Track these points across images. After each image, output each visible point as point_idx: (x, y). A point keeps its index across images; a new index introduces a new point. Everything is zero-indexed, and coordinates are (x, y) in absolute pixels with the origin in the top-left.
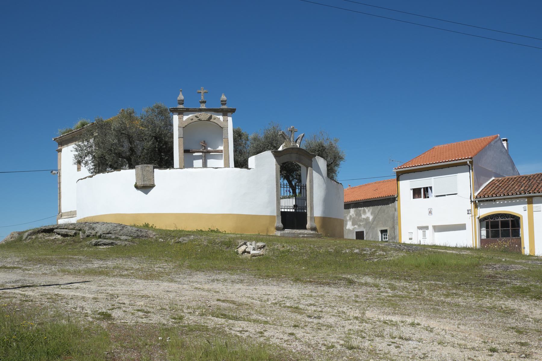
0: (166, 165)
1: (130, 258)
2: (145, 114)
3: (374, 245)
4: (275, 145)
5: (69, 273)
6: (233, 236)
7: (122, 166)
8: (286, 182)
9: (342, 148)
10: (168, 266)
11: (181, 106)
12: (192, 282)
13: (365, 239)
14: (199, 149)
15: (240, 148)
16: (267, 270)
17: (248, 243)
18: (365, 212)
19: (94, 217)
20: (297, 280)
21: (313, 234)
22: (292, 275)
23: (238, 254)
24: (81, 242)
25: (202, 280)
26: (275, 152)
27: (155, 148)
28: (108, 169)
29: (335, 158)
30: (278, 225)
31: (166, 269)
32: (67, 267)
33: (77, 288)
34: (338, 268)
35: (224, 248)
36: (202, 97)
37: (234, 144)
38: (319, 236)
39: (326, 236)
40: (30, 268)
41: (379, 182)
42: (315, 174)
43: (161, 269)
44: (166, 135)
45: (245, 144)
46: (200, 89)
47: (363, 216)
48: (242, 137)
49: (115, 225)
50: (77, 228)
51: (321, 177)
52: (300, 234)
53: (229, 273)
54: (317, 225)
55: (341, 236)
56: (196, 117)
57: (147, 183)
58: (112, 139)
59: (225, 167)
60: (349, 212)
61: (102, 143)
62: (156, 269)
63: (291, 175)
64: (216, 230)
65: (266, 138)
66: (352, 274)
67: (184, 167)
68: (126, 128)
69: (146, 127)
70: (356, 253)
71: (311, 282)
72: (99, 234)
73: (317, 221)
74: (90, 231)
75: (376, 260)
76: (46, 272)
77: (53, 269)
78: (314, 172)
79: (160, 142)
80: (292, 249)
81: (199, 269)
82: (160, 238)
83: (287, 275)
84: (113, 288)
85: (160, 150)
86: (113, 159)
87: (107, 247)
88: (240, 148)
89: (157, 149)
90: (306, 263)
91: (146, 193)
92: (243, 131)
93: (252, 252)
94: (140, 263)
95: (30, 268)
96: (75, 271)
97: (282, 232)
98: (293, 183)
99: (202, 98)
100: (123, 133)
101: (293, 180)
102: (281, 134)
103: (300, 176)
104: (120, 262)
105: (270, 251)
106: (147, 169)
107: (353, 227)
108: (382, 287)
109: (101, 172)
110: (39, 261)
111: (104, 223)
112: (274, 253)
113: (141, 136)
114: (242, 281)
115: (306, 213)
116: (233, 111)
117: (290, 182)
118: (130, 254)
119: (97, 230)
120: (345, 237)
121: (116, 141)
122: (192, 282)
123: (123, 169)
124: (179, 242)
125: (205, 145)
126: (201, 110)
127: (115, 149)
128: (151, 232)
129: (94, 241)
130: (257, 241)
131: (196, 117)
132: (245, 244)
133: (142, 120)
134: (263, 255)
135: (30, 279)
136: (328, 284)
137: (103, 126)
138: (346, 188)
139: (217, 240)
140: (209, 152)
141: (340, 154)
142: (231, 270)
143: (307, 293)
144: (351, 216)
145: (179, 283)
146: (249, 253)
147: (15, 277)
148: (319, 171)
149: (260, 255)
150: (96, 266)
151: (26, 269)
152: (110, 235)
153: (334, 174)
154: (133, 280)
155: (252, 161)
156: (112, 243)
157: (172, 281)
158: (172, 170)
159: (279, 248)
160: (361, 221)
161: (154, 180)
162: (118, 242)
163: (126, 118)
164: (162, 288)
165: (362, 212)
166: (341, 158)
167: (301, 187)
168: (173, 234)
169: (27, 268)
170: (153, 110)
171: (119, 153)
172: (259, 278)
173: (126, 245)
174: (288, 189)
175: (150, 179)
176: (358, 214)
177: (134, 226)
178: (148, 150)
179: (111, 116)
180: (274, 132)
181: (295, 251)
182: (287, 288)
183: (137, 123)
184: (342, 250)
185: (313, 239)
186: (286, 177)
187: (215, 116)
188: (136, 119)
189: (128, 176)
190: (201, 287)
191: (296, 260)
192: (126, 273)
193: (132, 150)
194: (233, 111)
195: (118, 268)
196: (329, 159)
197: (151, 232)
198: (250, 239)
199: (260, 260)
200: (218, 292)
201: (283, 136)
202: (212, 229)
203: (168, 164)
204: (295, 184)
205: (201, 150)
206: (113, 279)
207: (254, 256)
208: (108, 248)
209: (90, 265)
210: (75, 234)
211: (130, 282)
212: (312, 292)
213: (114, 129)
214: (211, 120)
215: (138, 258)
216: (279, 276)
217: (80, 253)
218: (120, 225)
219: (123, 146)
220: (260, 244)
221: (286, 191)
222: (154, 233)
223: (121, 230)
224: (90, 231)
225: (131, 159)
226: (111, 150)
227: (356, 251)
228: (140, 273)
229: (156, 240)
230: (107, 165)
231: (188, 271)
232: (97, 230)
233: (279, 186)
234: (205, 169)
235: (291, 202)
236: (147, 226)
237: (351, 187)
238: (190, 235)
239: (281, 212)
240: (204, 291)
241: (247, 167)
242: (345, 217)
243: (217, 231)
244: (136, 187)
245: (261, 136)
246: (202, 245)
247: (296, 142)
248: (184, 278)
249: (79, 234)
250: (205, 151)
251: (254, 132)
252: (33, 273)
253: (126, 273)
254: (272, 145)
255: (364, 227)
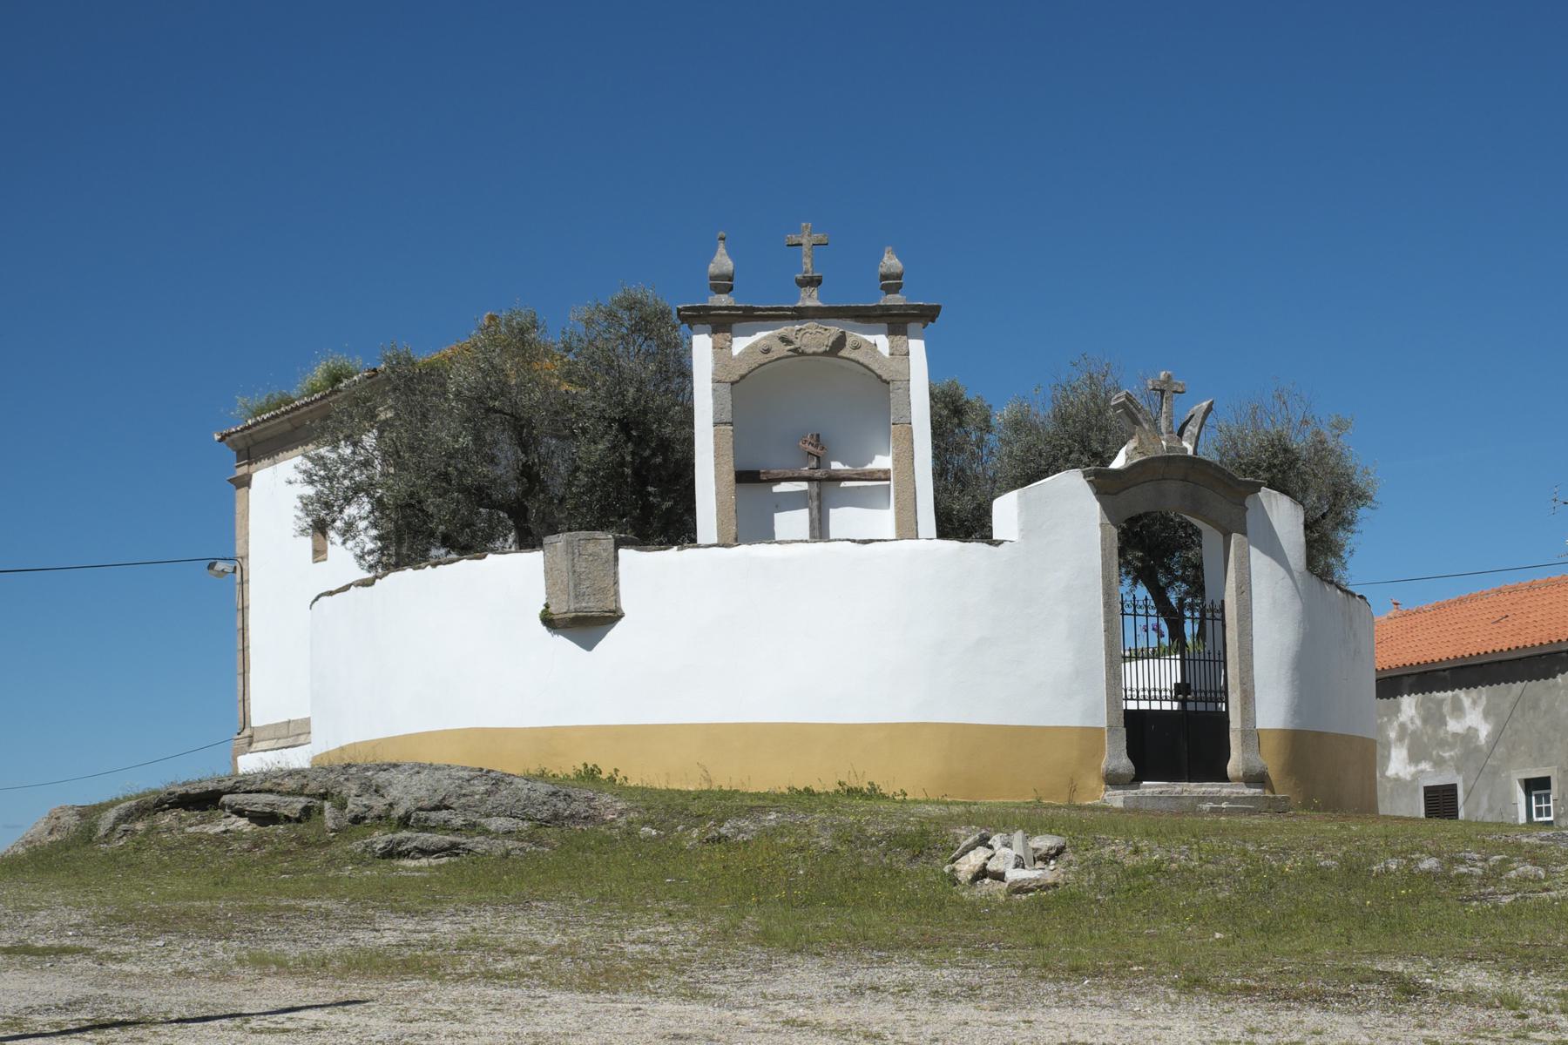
0: (663, 531)
1: (524, 903)
2: (581, 329)
3: (1502, 841)
4: (1096, 446)
5: (283, 967)
6: (934, 810)
7: (490, 538)
8: (1142, 592)
9: (1362, 456)
10: (678, 936)
11: (724, 300)
12: (775, 997)
13: (1462, 814)
14: (795, 471)
15: (958, 460)
16: (1072, 944)
17: (996, 840)
18: (1458, 709)
19: (379, 742)
20: (1194, 984)
21: (1253, 798)
22: (1175, 963)
23: (955, 882)
24: (329, 843)
25: (815, 990)
26: (1097, 474)
27: (622, 464)
28: (434, 552)
29: (1337, 494)
30: (1114, 764)
31: (671, 949)
32: (275, 946)
33: (316, 1029)
34: (1357, 934)
35: (901, 860)
36: (807, 264)
37: (935, 447)
38: (1278, 808)
39: (1305, 806)
40: (125, 949)
41: (1515, 589)
42: (1259, 561)
43: (648, 948)
44: (663, 412)
45: (980, 443)
46: (798, 231)
47: (1454, 726)
48: (966, 418)
49: (465, 774)
50: (313, 787)
51: (1281, 571)
52: (1202, 799)
53: (923, 961)
54: (1270, 761)
55: (1366, 806)
56: (785, 340)
57: (592, 605)
58: (450, 434)
59: (901, 537)
60: (1398, 710)
61: (412, 449)
62: (630, 949)
63: (1163, 565)
64: (866, 786)
65: (1062, 419)
66: (1414, 957)
67: (738, 541)
68: (504, 389)
69: (584, 382)
70: (1429, 872)
71: (1248, 991)
72: (399, 811)
73: (1269, 745)
74: (365, 800)
75: (1507, 900)
76: (190, 965)
77: (220, 954)
78: (1254, 552)
79: (641, 442)
80: (1172, 860)
81: (801, 946)
82: (644, 824)
83: (1153, 964)
84: (457, 1026)
85: (642, 474)
86: (455, 513)
87: (434, 862)
88: (958, 460)
89: (628, 471)
90: (1229, 914)
91: (589, 646)
92: (969, 395)
93: (1013, 875)
94: (563, 925)
95: (125, 949)
96: (305, 962)
97: (1131, 793)
98: (1173, 598)
99: (807, 267)
100: (490, 407)
101: (1170, 584)
102: (1122, 405)
103: (1199, 567)
104: (484, 921)
105: (1085, 868)
106: (591, 547)
107: (1412, 769)
108: (1533, 1006)
109: (408, 565)
110: (164, 923)
111: (419, 768)
112: (1099, 877)
113: (564, 420)
114: (971, 993)
115: (1224, 718)
116: (927, 314)
117: (1159, 594)
118: (526, 889)
119: (394, 793)
120: (1384, 808)
121: (465, 440)
122: (775, 997)
123: (494, 551)
124: (719, 839)
125: (819, 449)
126: (801, 314)
127: (462, 473)
128: (606, 798)
129: (380, 839)
130: (1032, 830)
131: (785, 340)
132: (984, 841)
133: (570, 357)
134: (1055, 885)
135: (127, 993)
136: (1319, 999)
137: (411, 384)
138: (1382, 613)
139: (870, 830)
140: (837, 478)
141: (1356, 480)
142: (929, 947)
143: (1234, 1037)
144: (1403, 726)
145: (723, 1001)
146: (999, 876)
147: (68, 989)
148: (1273, 549)
149: (1045, 887)
150: (390, 938)
151: (111, 957)
152: (444, 814)
153: (1332, 560)
154: (539, 991)
155: (1006, 510)
156: (454, 845)
157: (693, 994)
158: (689, 553)
159: (1119, 857)
160: (1442, 744)
161: (617, 593)
162: (479, 844)
163: (505, 349)
164: (653, 1022)
165: (1446, 709)
166: (1360, 497)
167: (1203, 613)
168: (696, 807)
169: (115, 950)
170: (611, 315)
171: (480, 489)
172: (1043, 978)
173: (508, 853)
174: (1152, 621)
175: (603, 590)
176: (1434, 718)
177: (542, 776)
178: (593, 472)
179: (447, 340)
180: (1094, 396)
181: (1183, 870)
182: (1154, 1015)
183: (549, 368)
184: (1372, 863)
185: (1256, 820)
186: (1144, 575)
187: (854, 336)
188: (546, 353)
189: (514, 578)
190: (810, 1016)
191: (1190, 905)
192: (509, 963)
193: (528, 474)
194: (927, 314)
195: (478, 945)
196: (1312, 498)
197: (606, 798)
198: (1004, 821)
199: (1043, 906)
200: (878, 1036)
201: (1130, 411)
202: (854, 784)
203: (673, 527)
204: (1181, 600)
205: (805, 470)
206: (457, 992)
207: (1019, 888)
208: (439, 867)
209: (364, 937)
210: (307, 811)
211: (524, 1002)
212: (1252, 1031)
213: (458, 394)
214: (843, 353)
215: (556, 906)
216: (1120, 971)
217: (325, 887)
218: (484, 773)
219: (492, 460)
220: (1044, 842)
221: (1146, 628)
222: (620, 806)
223: (488, 793)
224: (365, 800)
225: (526, 509)
226: (446, 477)
227: (1429, 864)
228: (566, 964)
229: (630, 833)
230: (432, 534)
231: (758, 954)
232: (394, 793)
233: (1115, 611)
234: (821, 546)
235: (1168, 672)
236: (591, 774)
237: (1403, 608)
238: (764, 810)
239: (1126, 711)
240: (822, 1033)
241: (986, 536)
242: (1381, 729)
243: (873, 794)
244: (548, 621)
245: (1043, 413)
246: (813, 850)
247: (1181, 433)
248: (742, 984)
249: (321, 811)
250: (818, 474)
251: (1012, 397)
252: (137, 970)
253: (509, 963)
254: (1085, 447)
255: (1458, 770)
